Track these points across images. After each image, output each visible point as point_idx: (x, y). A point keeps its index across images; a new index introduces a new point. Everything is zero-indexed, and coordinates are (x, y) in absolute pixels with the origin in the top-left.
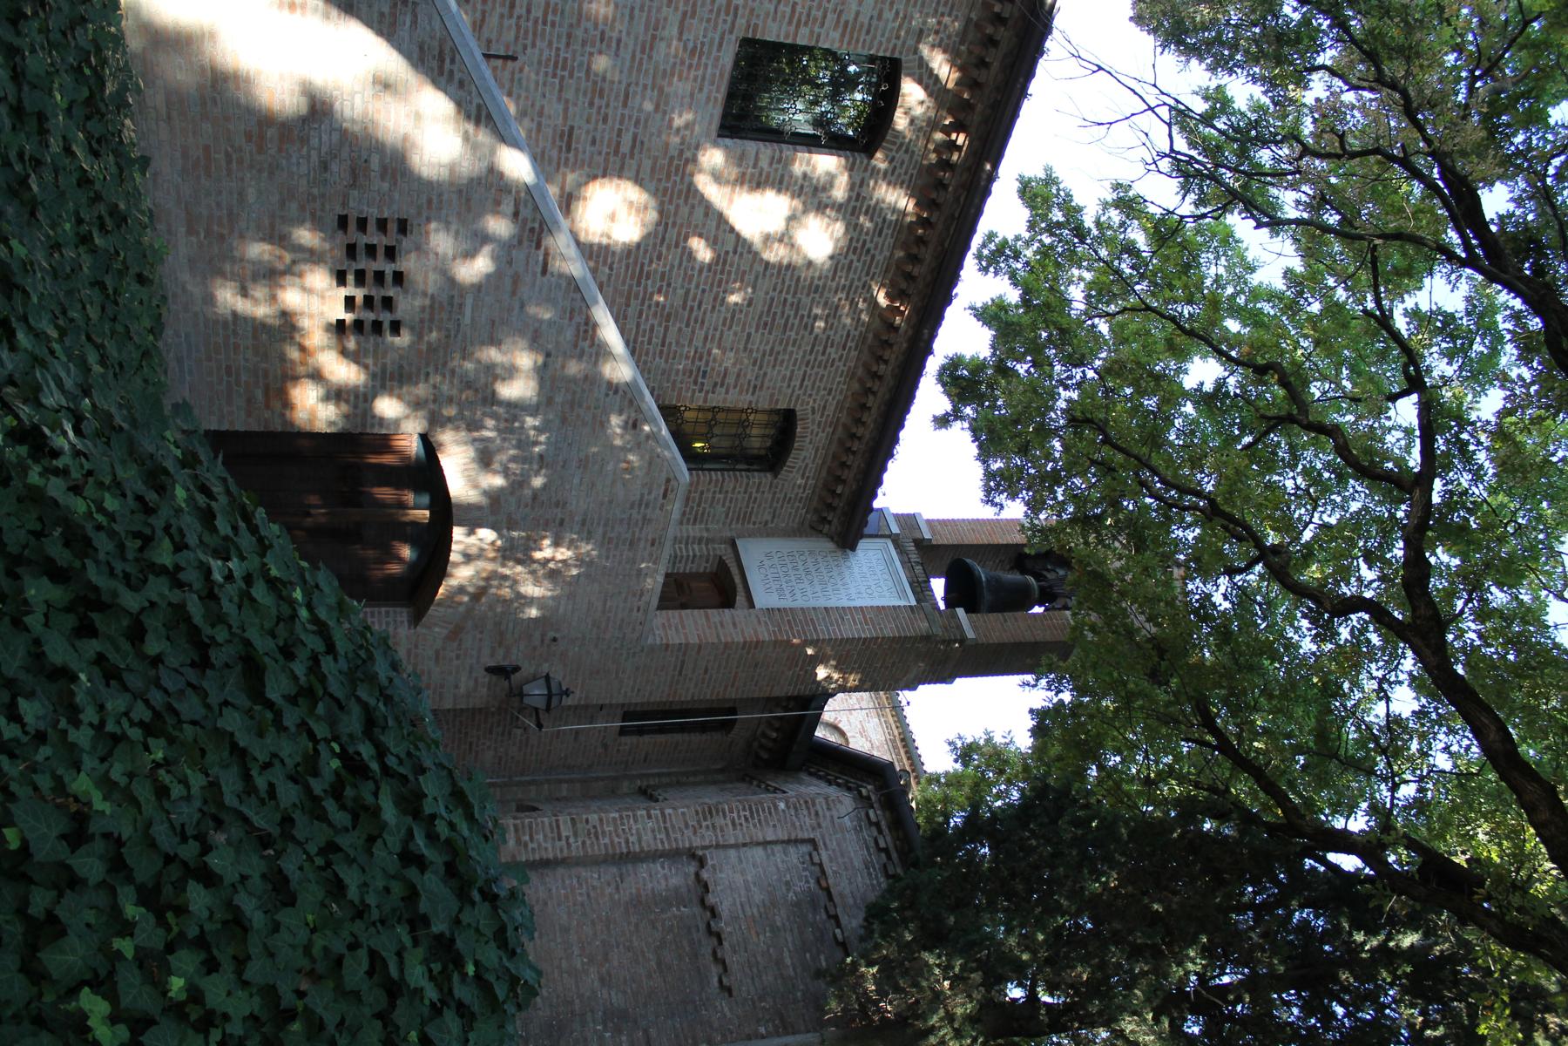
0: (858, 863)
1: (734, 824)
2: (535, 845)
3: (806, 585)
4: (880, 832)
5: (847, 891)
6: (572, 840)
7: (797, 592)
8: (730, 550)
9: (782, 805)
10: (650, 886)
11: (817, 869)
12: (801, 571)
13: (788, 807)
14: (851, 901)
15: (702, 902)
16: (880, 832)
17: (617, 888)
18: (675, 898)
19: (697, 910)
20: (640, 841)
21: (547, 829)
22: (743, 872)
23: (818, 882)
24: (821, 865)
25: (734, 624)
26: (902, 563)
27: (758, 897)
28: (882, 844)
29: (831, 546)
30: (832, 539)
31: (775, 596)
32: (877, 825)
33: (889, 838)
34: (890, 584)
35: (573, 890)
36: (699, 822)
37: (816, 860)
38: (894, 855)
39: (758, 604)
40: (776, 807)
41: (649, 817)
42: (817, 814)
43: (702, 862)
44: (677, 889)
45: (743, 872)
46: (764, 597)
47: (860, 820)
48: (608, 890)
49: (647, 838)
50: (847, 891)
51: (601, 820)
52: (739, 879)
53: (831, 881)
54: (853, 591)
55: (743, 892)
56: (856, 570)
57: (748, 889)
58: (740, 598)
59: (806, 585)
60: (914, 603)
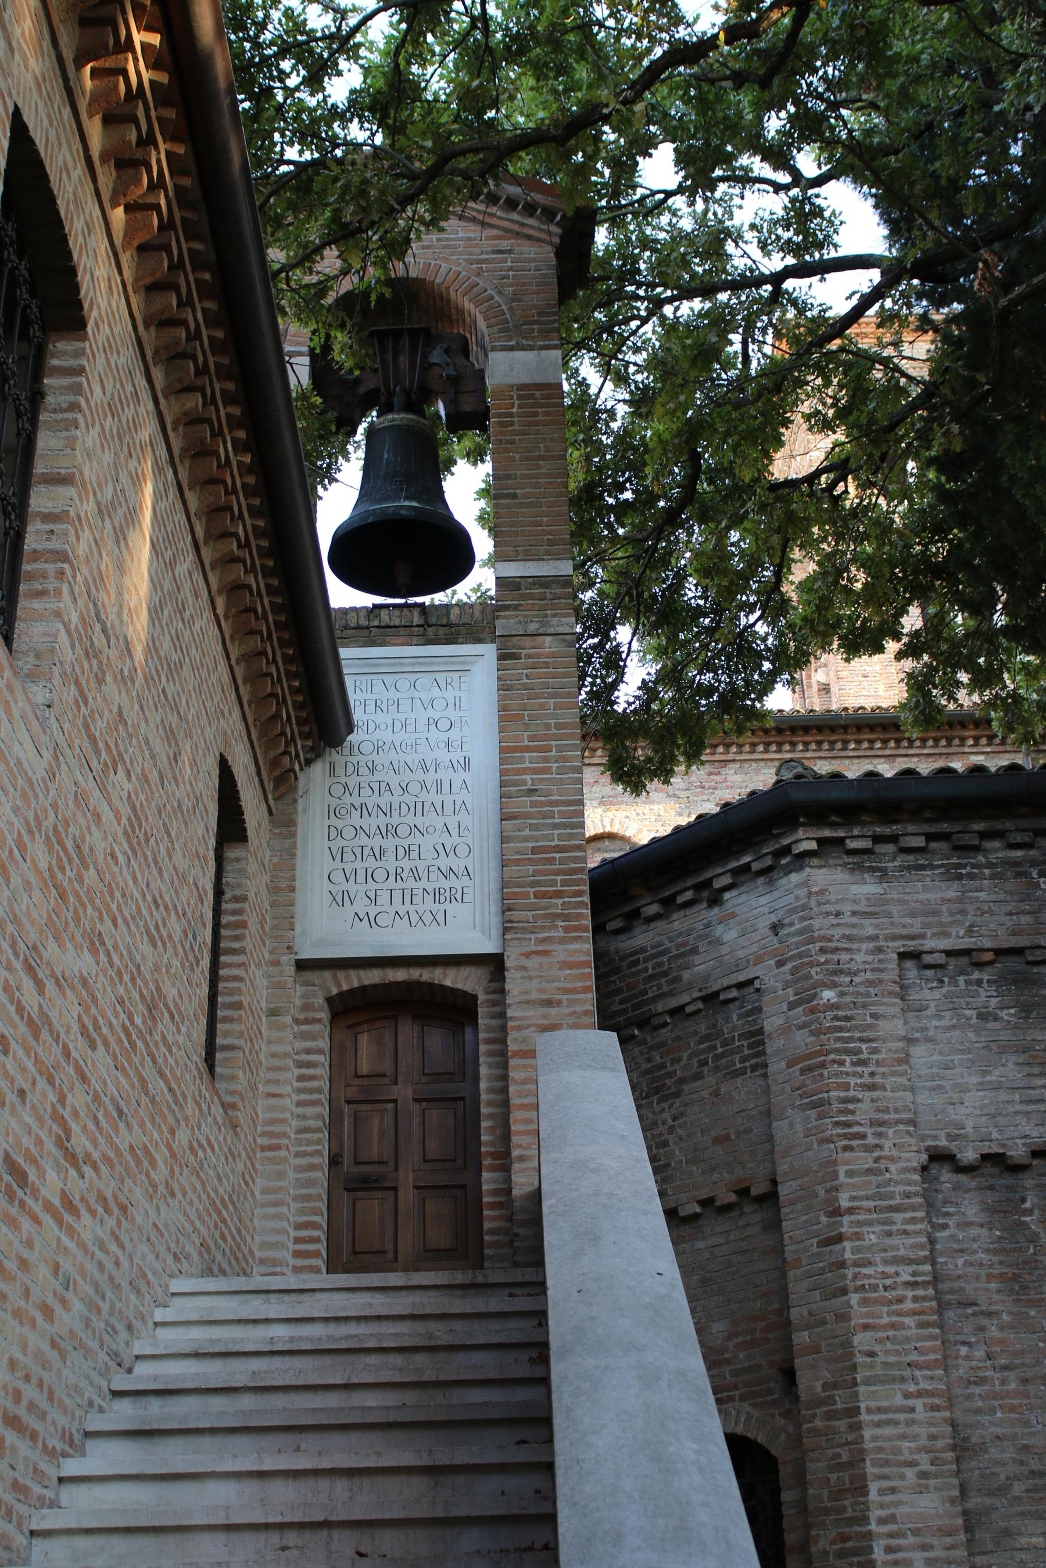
0: (952, 891)
1: (872, 1087)
2: (924, 1459)
3: (427, 843)
4: (893, 839)
5: (1008, 921)
6: (912, 1388)
7: (444, 862)
8: (313, 976)
9: (828, 995)
10: (981, 1255)
11: (953, 962)
12: (390, 843)
13: (833, 985)
14: (1025, 919)
15: (1018, 1169)
16: (893, 839)
17: (990, 1314)
18: (1005, 1212)
19: (1028, 1181)
20: (911, 1262)
21: (887, 1431)
22: (964, 1090)
23: (980, 965)
24: (949, 953)
25: (549, 1003)
26: (372, 644)
27: (1009, 1070)
28: (919, 842)
29: (318, 769)
30: (308, 762)
31: (452, 908)
32: (877, 839)
33: (911, 828)
34: (425, 680)
35: (995, 1396)
36: (869, 1149)
37: (938, 958)
38: (945, 827)
39: (488, 946)
40: (835, 1007)
41: (858, 1237)
42: (850, 938)
43: (939, 1157)
44: (987, 1208)
45: (964, 1090)
46: (465, 928)
47: (857, 868)
48: (993, 1332)
49: (902, 1246)
50: (1008, 921)
51: (866, 1327)
52: (972, 1098)
53: (987, 944)
54: (443, 756)
55: (1003, 1096)
56: (386, 736)
57: (998, 1087)
58: (450, 978)
59: (427, 843)
60: (488, 651)
